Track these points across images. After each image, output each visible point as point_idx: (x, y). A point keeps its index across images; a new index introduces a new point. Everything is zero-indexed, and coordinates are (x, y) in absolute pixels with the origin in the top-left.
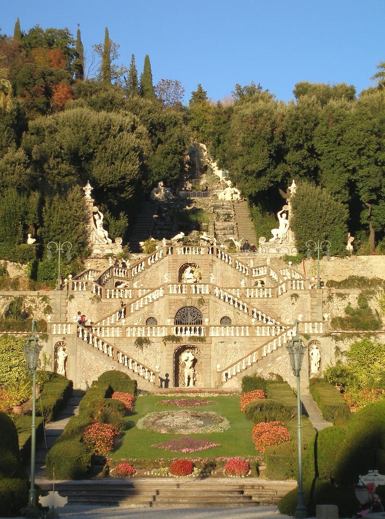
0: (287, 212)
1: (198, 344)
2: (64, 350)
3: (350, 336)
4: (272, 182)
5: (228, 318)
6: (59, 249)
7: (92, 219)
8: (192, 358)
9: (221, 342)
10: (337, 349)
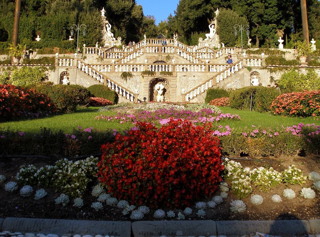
0: (214, 25)
1: (167, 77)
2: (68, 78)
3: (281, 69)
4: (204, 13)
7: (105, 27)
9: (184, 76)
10: (272, 78)
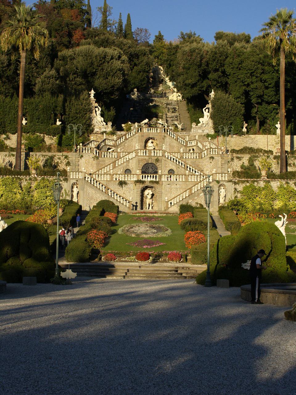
0: (209, 109)
1: (155, 185)
2: (77, 187)
3: (243, 182)
4: (200, 90)
5: (173, 170)
6: (75, 128)
7: (94, 111)
8: (151, 193)
9: (168, 184)
10: (235, 189)
